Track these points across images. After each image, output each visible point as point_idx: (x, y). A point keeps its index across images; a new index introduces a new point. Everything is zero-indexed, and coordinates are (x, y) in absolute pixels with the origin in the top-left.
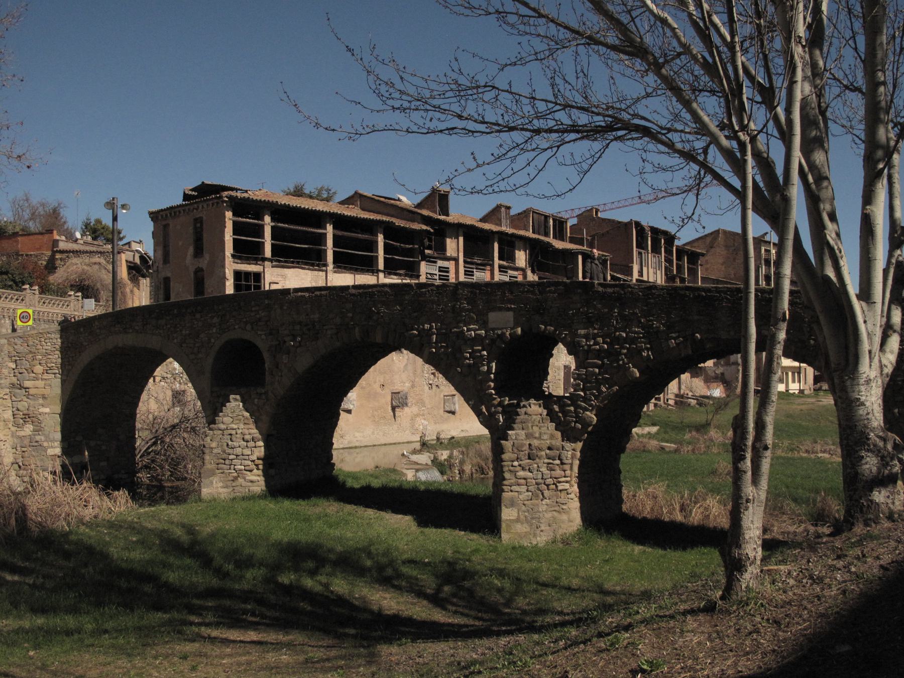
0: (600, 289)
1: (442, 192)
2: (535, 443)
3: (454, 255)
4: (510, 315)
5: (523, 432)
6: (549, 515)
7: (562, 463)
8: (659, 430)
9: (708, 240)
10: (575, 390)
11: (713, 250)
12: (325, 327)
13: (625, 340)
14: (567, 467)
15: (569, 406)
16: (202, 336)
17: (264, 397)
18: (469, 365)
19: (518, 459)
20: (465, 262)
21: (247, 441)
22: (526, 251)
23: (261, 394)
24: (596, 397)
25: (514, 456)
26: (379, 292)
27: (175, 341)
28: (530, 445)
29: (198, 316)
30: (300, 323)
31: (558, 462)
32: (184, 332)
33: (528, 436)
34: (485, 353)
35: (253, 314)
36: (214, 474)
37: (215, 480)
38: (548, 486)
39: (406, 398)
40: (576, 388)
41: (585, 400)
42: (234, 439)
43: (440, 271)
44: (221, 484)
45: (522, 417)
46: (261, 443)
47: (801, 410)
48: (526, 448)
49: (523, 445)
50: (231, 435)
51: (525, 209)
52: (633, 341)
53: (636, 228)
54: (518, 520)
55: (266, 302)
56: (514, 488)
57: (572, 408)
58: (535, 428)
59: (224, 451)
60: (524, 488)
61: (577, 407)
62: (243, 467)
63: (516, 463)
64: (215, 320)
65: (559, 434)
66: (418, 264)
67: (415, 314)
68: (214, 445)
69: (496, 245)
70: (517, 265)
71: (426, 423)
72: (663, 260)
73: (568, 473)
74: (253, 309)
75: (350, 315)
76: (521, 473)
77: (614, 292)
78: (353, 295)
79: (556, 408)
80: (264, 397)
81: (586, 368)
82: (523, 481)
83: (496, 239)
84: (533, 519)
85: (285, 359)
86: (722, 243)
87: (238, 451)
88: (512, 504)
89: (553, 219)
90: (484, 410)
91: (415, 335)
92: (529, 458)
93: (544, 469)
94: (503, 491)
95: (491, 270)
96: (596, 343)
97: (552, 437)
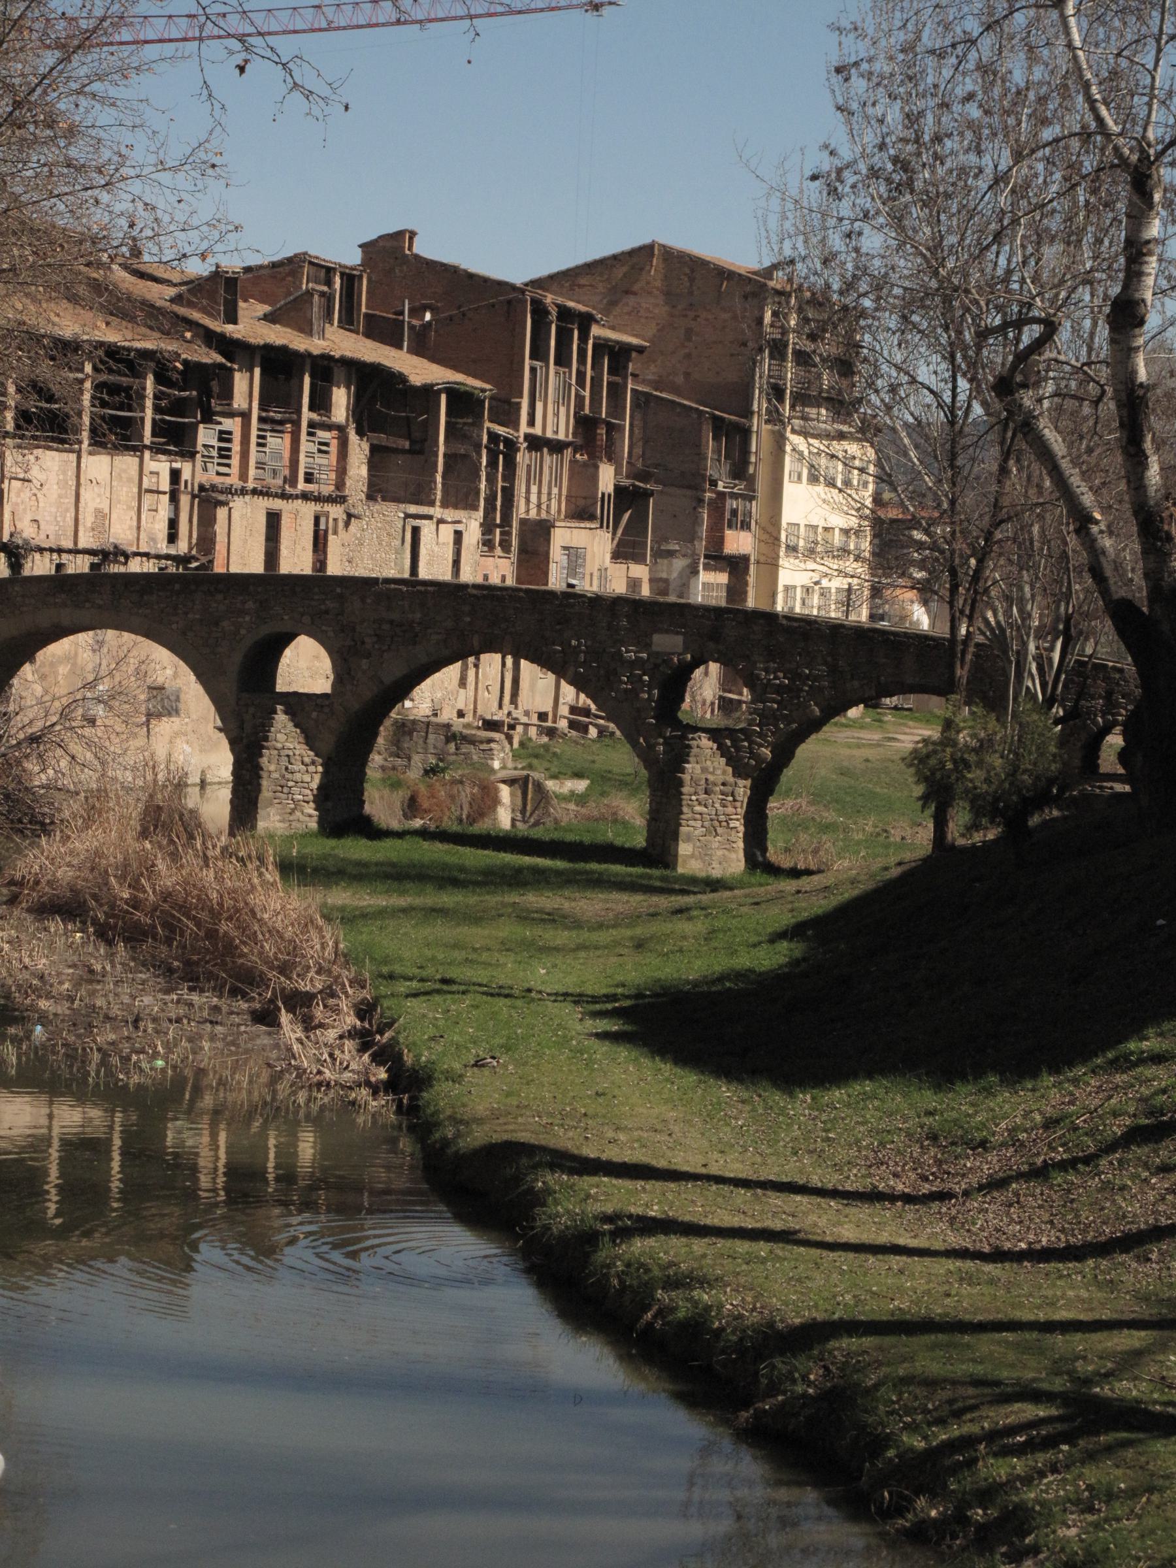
0: (784, 622)
1: (230, 275)
2: (711, 778)
3: (245, 406)
4: (679, 639)
5: (698, 766)
6: (720, 853)
7: (735, 800)
8: (588, 788)
9: (620, 272)
10: (749, 725)
11: (631, 300)
12: (429, 631)
13: (808, 677)
14: (739, 804)
15: (743, 741)
16: (225, 624)
17: (326, 710)
18: (626, 690)
19: (696, 793)
20: (261, 420)
21: (307, 765)
22: (348, 388)
23: (322, 706)
24: (772, 733)
25: (692, 790)
26: (510, 596)
27: (174, 626)
28: (707, 779)
29: (220, 597)
30: (391, 622)
31: (730, 798)
32: (190, 616)
33: (704, 770)
34: (646, 678)
35: (314, 603)
36: (271, 804)
37: (272, 811)
38: (720, 822)
39: (178, 699)
40: (751, 723)
41: (761, 735)
42: (293, 761)
43: (221, 440)
44: (278, 818)
45: (694, 751)
46: (320, 769)
47: (867, 760)
48: (703, 782)
49: (700, 780)
50: (288, 756)
51: (290, 254)
52: (816, 678)
53: (533, 312)
54: (692, 856)
55: (338, 590)
56: (691, 823)
57: (746, 744)
58: (709, 763)
59: (283, 777)
60: (699, 824)
61: (751, 742)
62: (301, 797)
63: (694, 798)
64: (250, 605)
65: (730, 770)
66: (194, 428)
67: (558, 627)
68: (272, 768)
69: (307, 380)
70: (334, 419)
71: (188, 749)
72: (573, 381)
73: (739, 810)
74: (316, 597)
75: (468, 619)
76: (698, 808)
77: (800, 627)
78: (474, 596)
79: (728, 742)
80: (326, 710)
81: (763, 702)
82: (698, 816)
83: (308, 367)
84: (704, 854)
85: (365, 664)
86: (658, 284)
87: (298, 776)
88: (688, 839)
89: (342, 274)
90: (641, 740)
91: (556, 652)
92: (706, 793)
93: (717, 805)
94: (680, 825)
95: (292, 433)
96: (776, 678)
97: (724, 773)
